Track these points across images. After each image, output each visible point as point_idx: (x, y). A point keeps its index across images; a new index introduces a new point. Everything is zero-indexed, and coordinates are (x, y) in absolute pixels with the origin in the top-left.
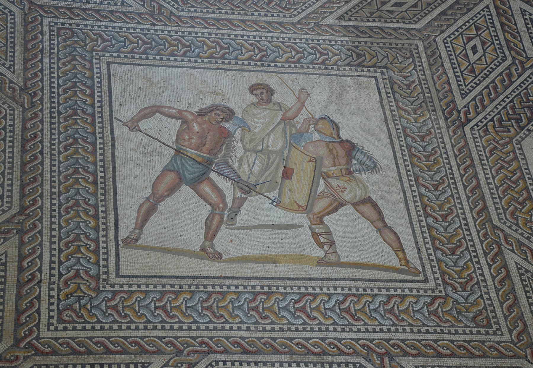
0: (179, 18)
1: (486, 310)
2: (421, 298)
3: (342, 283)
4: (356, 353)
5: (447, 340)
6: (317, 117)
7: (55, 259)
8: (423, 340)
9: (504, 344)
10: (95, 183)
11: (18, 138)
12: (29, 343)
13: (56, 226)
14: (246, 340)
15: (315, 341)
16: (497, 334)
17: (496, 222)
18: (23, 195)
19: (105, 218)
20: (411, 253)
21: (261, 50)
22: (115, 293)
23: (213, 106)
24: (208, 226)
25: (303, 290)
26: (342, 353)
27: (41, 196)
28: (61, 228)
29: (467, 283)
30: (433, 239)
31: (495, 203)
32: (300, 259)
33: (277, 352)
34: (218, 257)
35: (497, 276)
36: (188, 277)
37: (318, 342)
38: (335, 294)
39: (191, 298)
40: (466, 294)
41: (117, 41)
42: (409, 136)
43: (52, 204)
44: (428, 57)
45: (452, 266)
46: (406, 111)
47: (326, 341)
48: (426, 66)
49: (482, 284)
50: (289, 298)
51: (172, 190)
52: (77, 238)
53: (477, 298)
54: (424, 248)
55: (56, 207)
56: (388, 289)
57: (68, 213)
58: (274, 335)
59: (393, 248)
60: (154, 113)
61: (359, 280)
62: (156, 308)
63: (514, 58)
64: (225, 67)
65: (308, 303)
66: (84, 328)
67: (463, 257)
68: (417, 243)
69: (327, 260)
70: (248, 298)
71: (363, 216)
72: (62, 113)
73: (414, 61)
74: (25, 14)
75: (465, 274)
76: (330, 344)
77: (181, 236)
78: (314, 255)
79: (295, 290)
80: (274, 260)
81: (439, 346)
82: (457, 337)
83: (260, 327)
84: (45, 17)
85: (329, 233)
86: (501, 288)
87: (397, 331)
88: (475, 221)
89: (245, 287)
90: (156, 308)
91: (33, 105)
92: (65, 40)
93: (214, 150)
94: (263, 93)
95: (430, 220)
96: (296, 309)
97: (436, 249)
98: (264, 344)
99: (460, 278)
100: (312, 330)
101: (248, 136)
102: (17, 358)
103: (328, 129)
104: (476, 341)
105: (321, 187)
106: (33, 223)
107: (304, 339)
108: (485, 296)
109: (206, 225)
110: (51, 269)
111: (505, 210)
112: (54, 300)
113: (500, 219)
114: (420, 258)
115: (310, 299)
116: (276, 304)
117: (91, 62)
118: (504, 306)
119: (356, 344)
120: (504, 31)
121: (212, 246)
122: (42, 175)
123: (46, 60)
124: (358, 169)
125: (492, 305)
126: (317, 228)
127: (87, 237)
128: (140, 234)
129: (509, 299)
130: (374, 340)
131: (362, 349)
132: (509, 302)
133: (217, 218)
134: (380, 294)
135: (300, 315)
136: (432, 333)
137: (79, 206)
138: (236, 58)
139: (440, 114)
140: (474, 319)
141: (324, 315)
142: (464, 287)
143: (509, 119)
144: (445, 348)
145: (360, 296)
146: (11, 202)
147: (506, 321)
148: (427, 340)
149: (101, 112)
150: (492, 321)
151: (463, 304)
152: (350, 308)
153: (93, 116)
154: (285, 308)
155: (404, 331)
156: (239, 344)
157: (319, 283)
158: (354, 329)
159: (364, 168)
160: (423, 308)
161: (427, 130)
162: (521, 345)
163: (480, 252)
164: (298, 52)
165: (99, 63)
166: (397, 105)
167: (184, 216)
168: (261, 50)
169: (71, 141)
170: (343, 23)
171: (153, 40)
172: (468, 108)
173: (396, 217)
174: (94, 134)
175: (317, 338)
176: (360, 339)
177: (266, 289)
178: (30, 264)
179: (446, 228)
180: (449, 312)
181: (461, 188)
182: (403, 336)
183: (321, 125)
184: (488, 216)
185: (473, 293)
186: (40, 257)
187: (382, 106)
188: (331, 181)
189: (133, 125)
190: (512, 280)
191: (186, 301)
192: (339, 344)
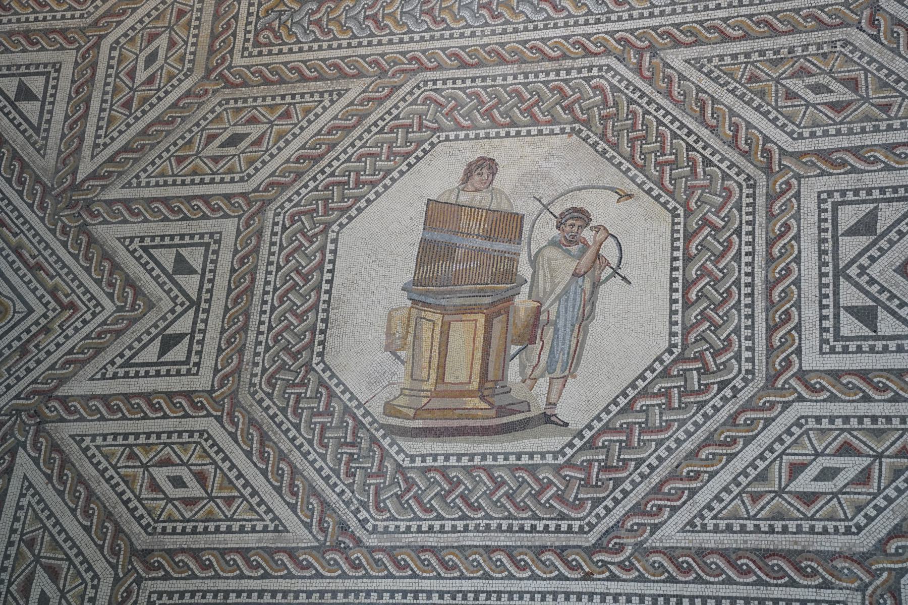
4: (607, 52)
12: (220, 73)
26: (589, 53)
33: (503, 61)
62: (366, 17)
66: (280, 52)
81: (729, 26)
83: (488, 30)
87: (674, 12)
98: (489, 53)
102: (206, 91)
130: (637, 29)
155: (684, 11)
156: (457, 56)
158: (614, 17)
176: (618, 31)
182: (678, 19)
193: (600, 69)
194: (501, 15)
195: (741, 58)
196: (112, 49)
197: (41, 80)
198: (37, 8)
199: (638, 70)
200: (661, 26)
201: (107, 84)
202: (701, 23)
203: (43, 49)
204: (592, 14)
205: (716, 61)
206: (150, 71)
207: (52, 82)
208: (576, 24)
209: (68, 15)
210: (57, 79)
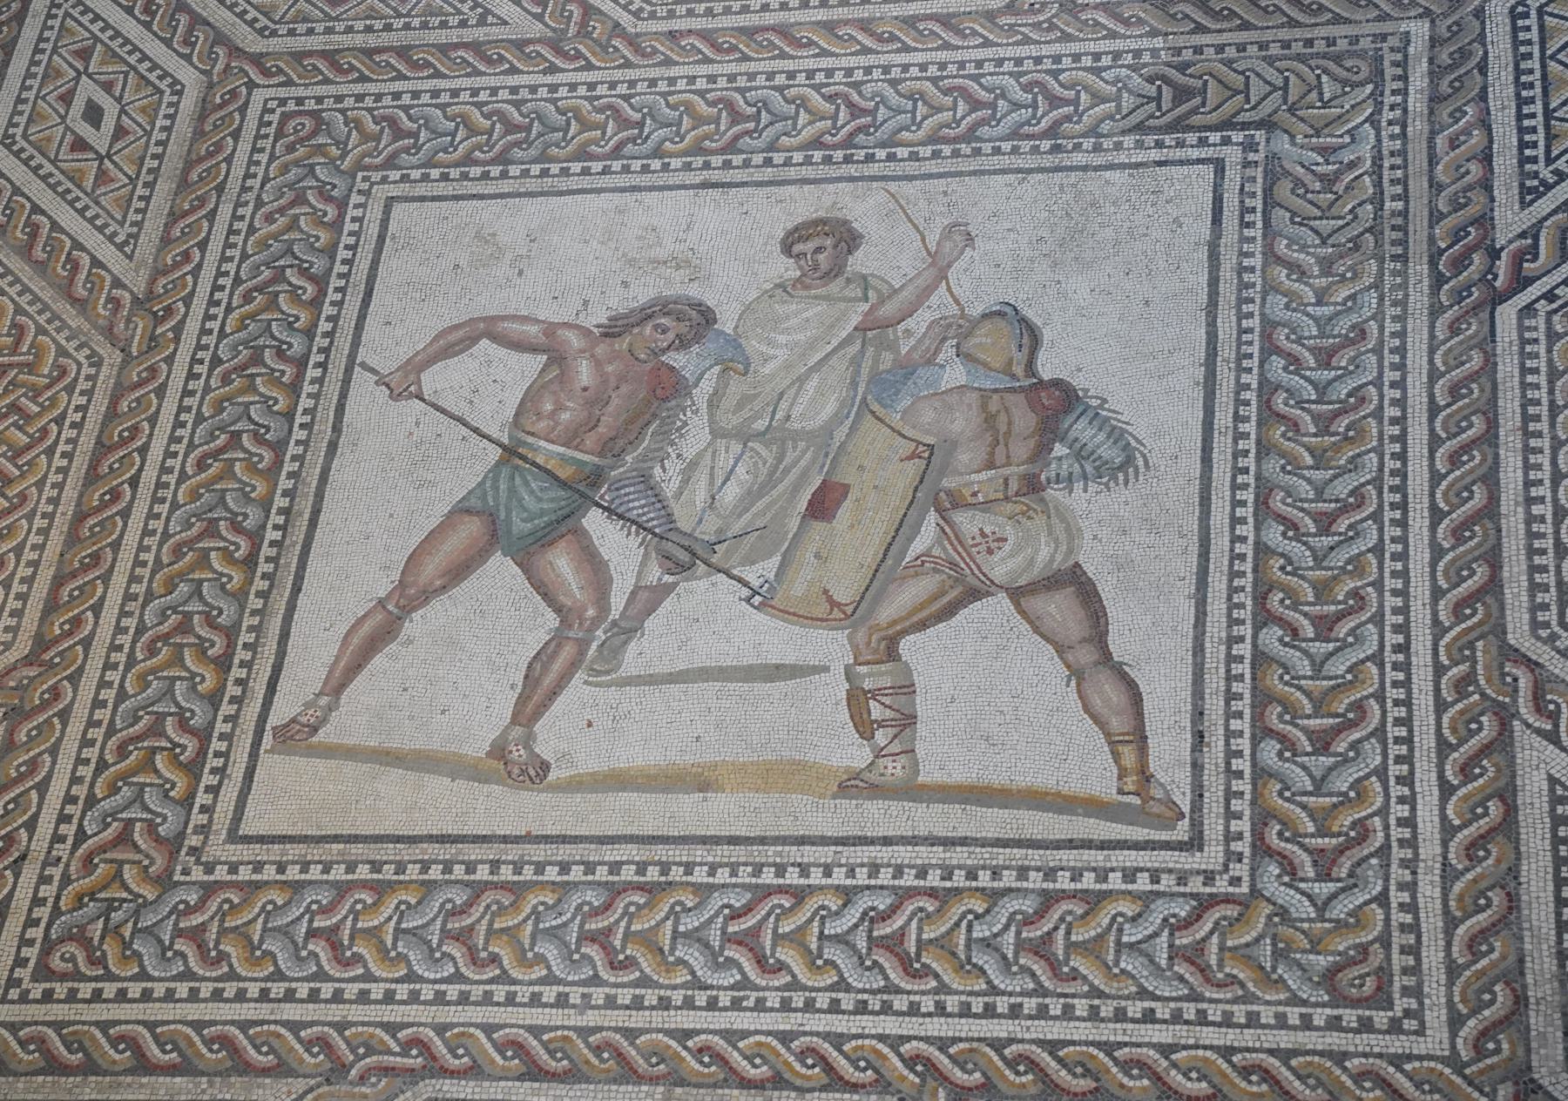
1: (1387, 946)
2: (1159, 902)
3: (903, 854)
5: (1211, 1048)
8: (1126, 1044)
9: (1417, 1064)
11: (87, 442)
14: (545, 1037)
15: (759, 1044)
16: (1401, 1031)
17: (1518, 633)
35: (1465, 825)
36: (431, 839)
37: (768, 1045)
38: (868, 887)
39: (419, 903)
40: (1324, 889)
41: (433, 132)
42: (1278, 351)
45: (1305, 793)
47: (795, 1044)
53: (1366, 903)
54: (1221, 731)
56: (1050, 873)
59: (1108, 735)
61: (964, 841)
65: (772, 919)
67: (1354, 759)
68: (1199, 714)
69: (873, 777)
70: (589, 903)
71: (1036, 630)
72: (221, 362)
74: (211, 86)
75: (1346, 820)
77: (443, 712)
78: (835, 762)
79: (745, 875)
80: (701, 782)
81: (1174, 1065)
84: (258, 86)
86: (1467, 870)
87: (1042, 1013)
95: (1271, 637)
96: (728, 939)
97: (1262, 732)
99: (1321, 832)
104: (1314, 1052)
109: (526, 677)
114: (1197, 767)
115: (781, 906)
116: (669, 923)
118: (1461, 930)
119: (891, 1055)
121: (528, 741)
124: (1064, 473)
126: (870, 675)
129: (1488, 905)
130: (955, 1040)
131: (906, 1072)
132: (1481, 917)
133: (568, 651)
134: (1018, 890)
135: (737, 956)
136: (1165, 1022)
140: (1331, 974)
141: (813, 961)
142: (1325, 865)
144: (1194, 1075)
147: (1450, 983)
148: (1139, 1045)
149: (326, 351)
151: (1306, 925)
155: (1068, 1013)
157: (826, 854)
158: (900, 1003)
159: (1089, 468)
160: (1156, 935)
161: (1353, 327)
162: (1481, 1072)
165: (363, 206)
171: (539, 117)
172: (1536, 238)
175: (769, 1033)
176: (909, 1039)
177: (653, 874)
178: (11, 806)
179: (1323, 663)
180: (1244, 954)
182: (1055, 1031)
184: (1495, 613)
185: (1355, 885)
189: (404, 385)
190: (1518, 841)
191: (402, 912)
192: (835, 1054)
194: (630, 963)
200: (1011, 1041)
202: (1108, 1048)
204: (848, 988)
208: (809, 1006)
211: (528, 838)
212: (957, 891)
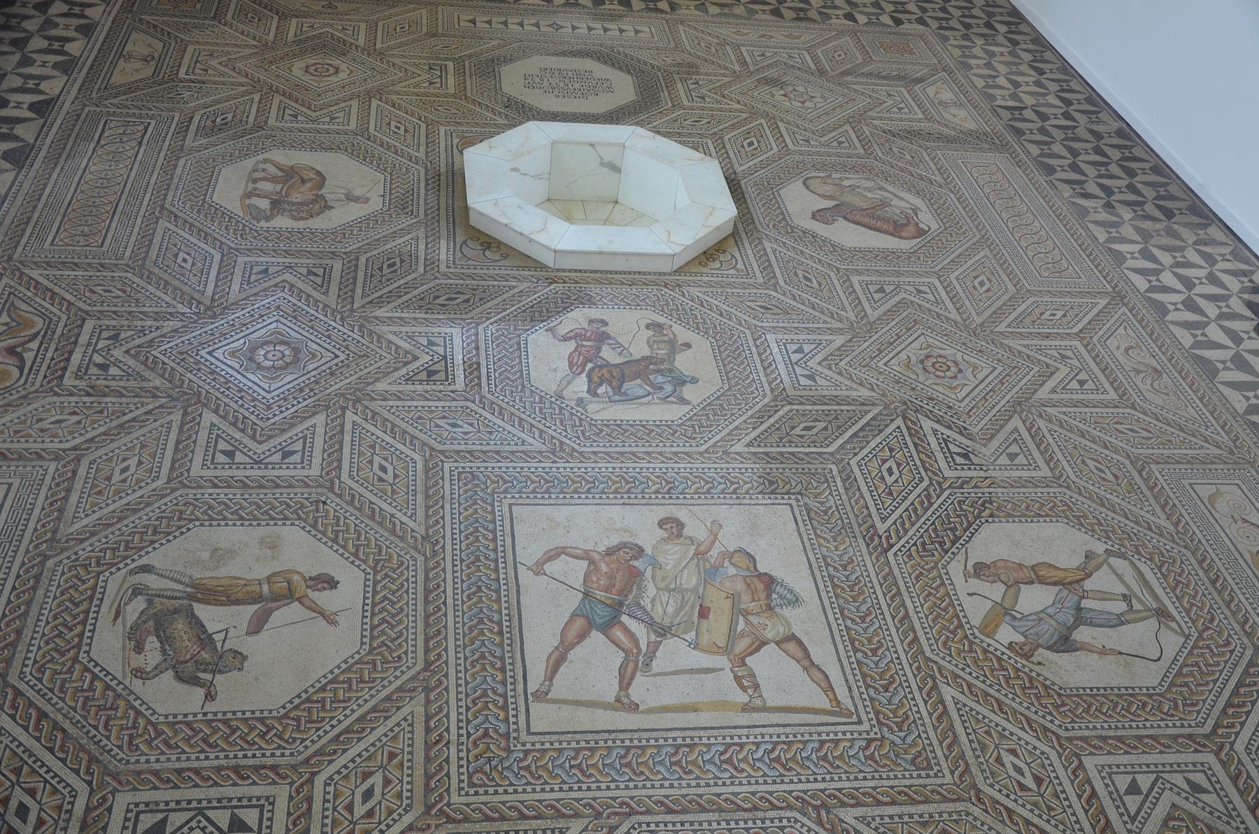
0: (581, 453)
3: (771, 730)
4: (790, 807)
6: (732, 550)
7: (463, 717)
10: (500, 633)
11: (420, 588)
12: (440, 810)
13: (462, 682)
17: (928, 654)
18: (427, 650)
19: (513, 670)
20: (842, 692)
21: (668, 483)
22: (527, 752)
23: (621, 543)
24: (622, 675)
25: (728, 740)
27: (446, 650)
28: (467, 683)
29: (903, 722)
30: (864, 676)
31: (926, 633)
32: (723, 705)
33: (704, 810)
34: (635, 707)
40: (903, 734)
43: (457, 658)
44: (844, 481)
46: (824, 539)
48: (842, 490)
49: (919, 722)
50: (714, 749)
51: (582, 636)
52: (484, 694)
55: (461, 661)
56: (819, 734)
57: (474, 667)
58: (700, 791)
60: (559, 555)
61: (789, 725)
62: (571, 767)
63: (930, 479)
64: (631, 501)
66: (496, 792)
68: (847, 681)
73: (829, 486)
76: (761, 798)
79: (720, 740)
82: (896, 782)
83: (684, 783)
85: (753, 675)
87: (832, 780)
88: (907, 654)
89: (666, 740)
90: (571, 767)
91: (435, 553)
92: (465, 484)
93: (624, 592)
94: (672, 527)
95: (859, 655)
96: (722, 762)
97: (868, 686)
98: (690, 802)
99: (895, 717)
100: (740, 784)
101: (659, 574)
102: (429, 826)
103: (744, 562)
105: (741, 625)
106: (439, 680)
107: (733, 794)
108: (924, 736)
110: (459, 728)
111: (937, 641)
112: (464, 762)
113: (932, 651)
117: (492, 505)
120: (918, 451)
121: (628, 696)
122: (445, 627)
123: (447, 506)
125: (931, 745)
127: (495, 692)
128: (550, 686)
133: (631, 665)
137: (485, 658)
138: (643, 492)
139: (861, 540)
140: (913, 760)
141: (753, 767)
142: (900, 726)
143: (932, 543)
145: (790, 744)
146: (416, 658)
149: (504, 557)
150: (933, 762)
152: (781, 757)
153: (496, 561)
154: (711, 761)
155: (840, 779)
156: (662, 803)
157: (745, 731)
158: (786, 780)
163: (914, 687)
164: (707, 482)
166: (815, 534)
167: (596, 664)
168: (668, 483)
169: (474, 589)
170: (752, 449)
173: (823, 653)
174: (498, 580)
177: (688, 741)
180: (886, 756)
181: (889, 619)
182: (839, 785)
183: (736, 558)
186: (447, 716)
187: (800, 534)
188: (750, 618)
189: (538, 569)
193: (789, 821)
195: (897, 819)
196: (326, 784)
197: (256, 812)
198: (245, 746)
199: (820, 823)
201: (325, 817)
203: (254, 783)
205: (878, 819)
206: (369, 805)
207: (266, 815)
209: (278, 753)
210: (272, 811)
211: (639, 730)
212: (792, 742)
